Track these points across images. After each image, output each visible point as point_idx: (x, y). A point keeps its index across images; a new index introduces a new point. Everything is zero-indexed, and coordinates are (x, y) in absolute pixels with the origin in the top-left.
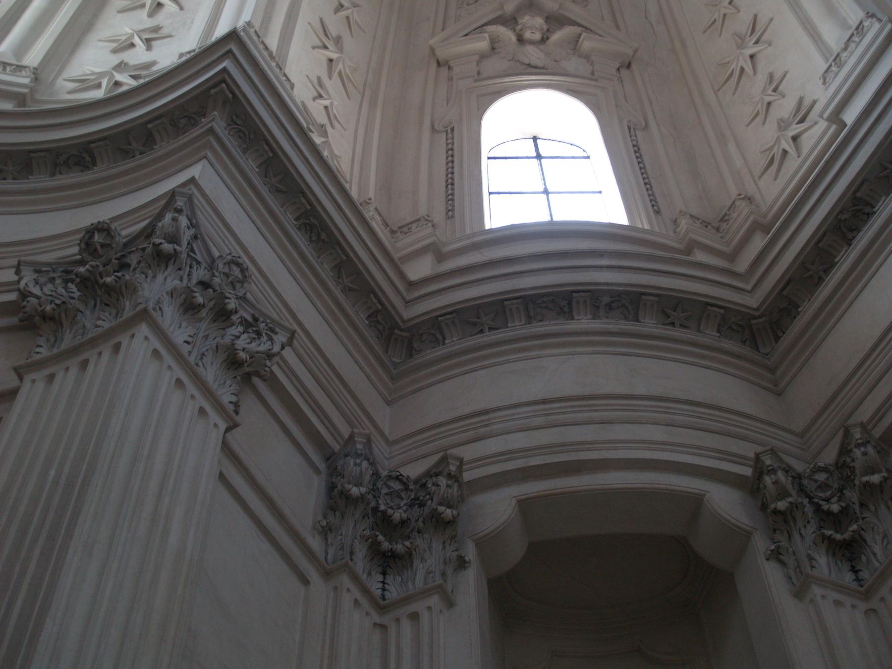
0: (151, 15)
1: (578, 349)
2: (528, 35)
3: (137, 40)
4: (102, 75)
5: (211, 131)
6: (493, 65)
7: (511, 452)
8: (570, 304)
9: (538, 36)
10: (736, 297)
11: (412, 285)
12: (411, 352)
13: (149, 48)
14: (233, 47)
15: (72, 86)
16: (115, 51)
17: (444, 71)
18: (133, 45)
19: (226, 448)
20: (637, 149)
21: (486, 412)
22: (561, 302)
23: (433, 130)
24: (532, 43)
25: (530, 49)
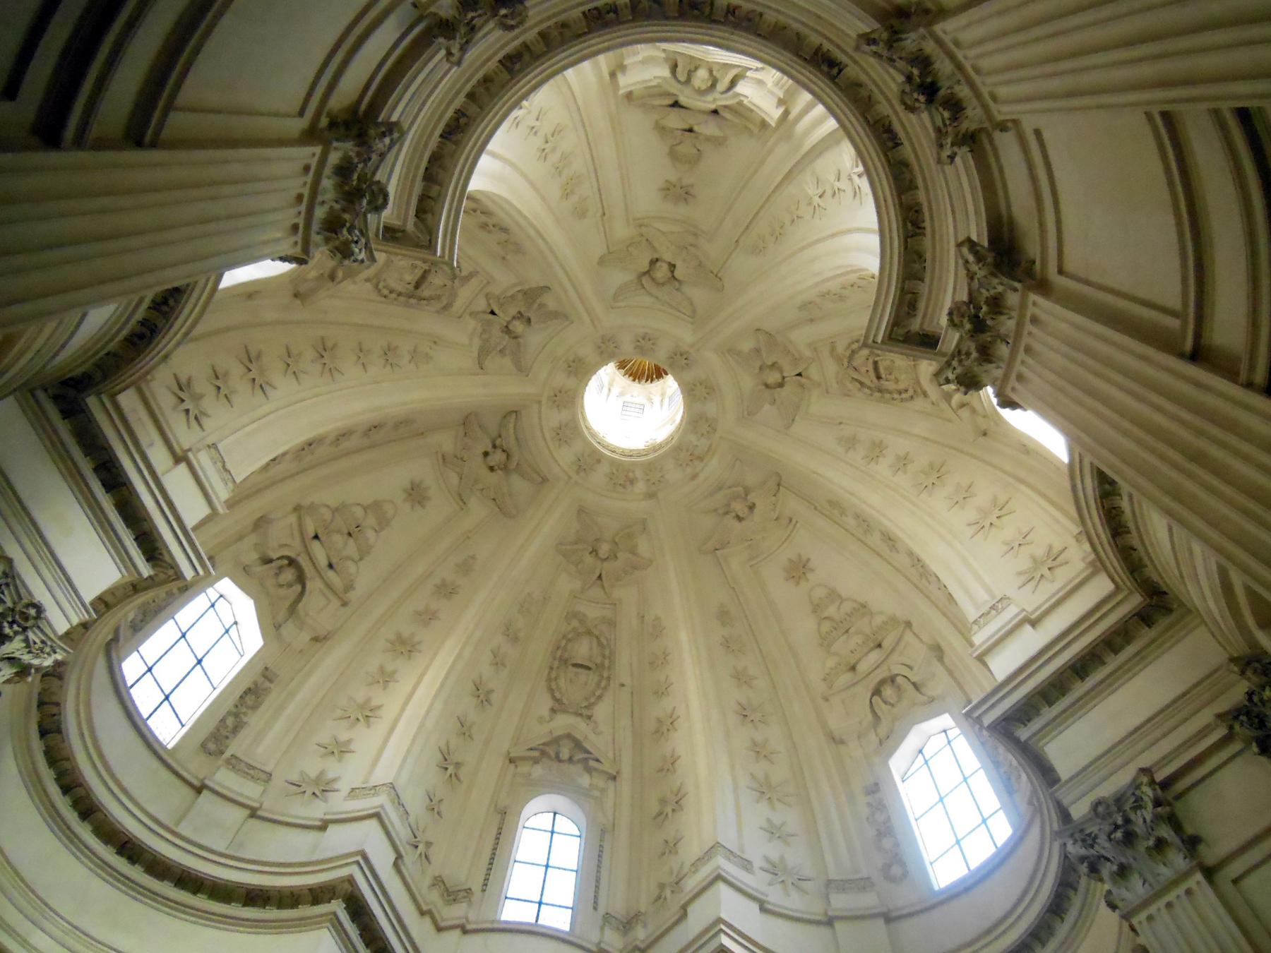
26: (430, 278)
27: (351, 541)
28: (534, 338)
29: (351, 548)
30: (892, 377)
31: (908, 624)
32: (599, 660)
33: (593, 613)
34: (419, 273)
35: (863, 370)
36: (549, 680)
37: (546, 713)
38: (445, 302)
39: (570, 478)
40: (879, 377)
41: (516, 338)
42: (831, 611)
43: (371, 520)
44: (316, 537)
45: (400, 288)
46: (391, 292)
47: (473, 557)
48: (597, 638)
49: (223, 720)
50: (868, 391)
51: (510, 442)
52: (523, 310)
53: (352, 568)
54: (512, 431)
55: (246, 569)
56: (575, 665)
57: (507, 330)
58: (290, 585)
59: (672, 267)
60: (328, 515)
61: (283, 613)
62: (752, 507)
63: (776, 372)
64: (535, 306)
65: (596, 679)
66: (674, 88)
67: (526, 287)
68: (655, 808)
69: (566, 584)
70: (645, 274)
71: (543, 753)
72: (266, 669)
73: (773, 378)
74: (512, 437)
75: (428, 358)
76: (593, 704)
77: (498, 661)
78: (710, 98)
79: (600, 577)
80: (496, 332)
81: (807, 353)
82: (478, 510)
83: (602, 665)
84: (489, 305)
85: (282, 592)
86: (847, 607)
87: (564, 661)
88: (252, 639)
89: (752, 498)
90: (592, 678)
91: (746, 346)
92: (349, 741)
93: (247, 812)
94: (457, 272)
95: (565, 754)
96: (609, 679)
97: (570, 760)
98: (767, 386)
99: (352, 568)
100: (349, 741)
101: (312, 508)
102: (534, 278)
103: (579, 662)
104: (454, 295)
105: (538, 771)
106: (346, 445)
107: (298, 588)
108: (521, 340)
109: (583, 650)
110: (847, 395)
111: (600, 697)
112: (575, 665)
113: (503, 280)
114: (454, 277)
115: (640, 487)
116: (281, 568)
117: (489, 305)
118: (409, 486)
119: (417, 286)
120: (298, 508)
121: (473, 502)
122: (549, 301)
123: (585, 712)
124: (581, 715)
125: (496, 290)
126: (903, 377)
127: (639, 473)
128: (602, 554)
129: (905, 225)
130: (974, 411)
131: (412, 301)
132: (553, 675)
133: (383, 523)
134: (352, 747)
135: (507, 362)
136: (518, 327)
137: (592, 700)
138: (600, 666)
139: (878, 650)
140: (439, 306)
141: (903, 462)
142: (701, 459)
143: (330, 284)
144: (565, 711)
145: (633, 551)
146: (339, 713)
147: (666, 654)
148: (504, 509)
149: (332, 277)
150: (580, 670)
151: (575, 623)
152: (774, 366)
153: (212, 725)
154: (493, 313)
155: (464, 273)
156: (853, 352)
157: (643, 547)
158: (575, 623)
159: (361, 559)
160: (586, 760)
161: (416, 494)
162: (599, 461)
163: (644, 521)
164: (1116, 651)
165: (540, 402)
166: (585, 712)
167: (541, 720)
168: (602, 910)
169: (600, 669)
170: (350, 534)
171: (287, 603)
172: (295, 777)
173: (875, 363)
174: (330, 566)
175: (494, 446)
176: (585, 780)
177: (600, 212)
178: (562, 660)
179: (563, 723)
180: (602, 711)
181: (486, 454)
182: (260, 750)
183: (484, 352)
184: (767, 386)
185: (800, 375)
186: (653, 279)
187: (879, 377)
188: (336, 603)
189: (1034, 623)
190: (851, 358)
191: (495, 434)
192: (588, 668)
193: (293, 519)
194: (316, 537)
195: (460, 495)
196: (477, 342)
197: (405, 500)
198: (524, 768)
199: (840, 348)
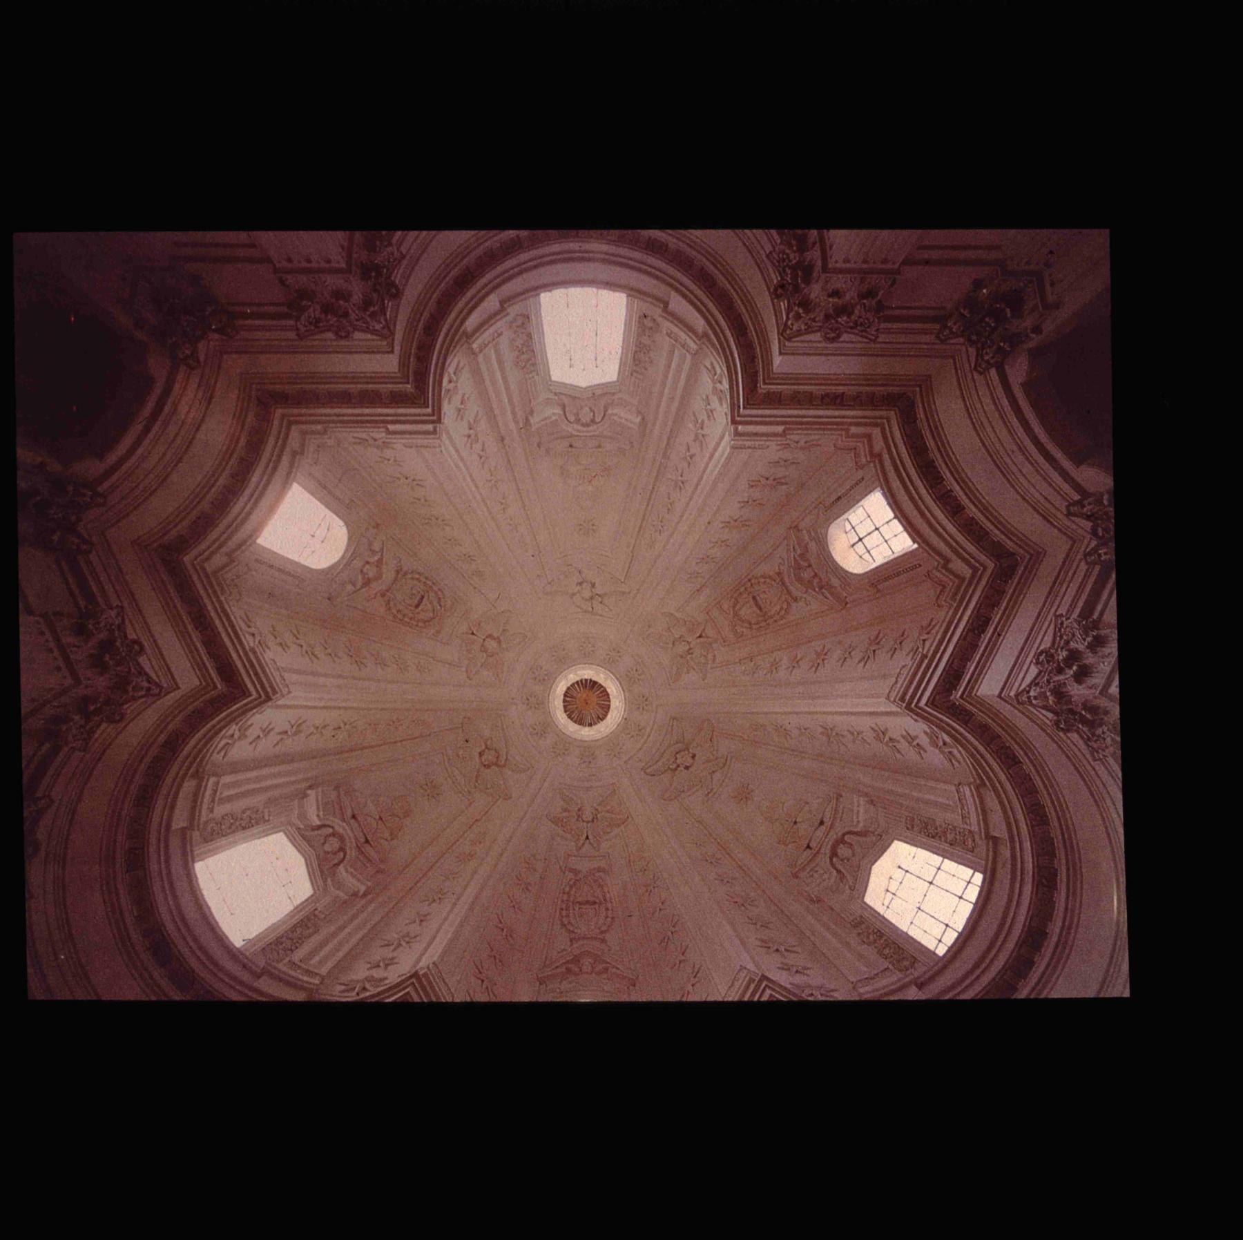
2: (367, 566)
15: (461, 365)
19: (268, 260)
21: (209, 403)
37: (801, 604)
40: (423, 597)
54: (660, 763)
56: (760, 609)
65: (757, 587)
66: (352, 854)
70: (496, 765)
71: (821, 588)
73: (491, 645)
76: (770, 577)
77: (795, 663)
78: (341, 831)
95: (806, 575)
97: (810, 566)
98: (499, 642)
103: (755, 609)
105: (835, 582)
109: (747, 611)
111: (764, 576)
130: (370, 544)
132: (777, 617)
136: (587, 815)
144: (789, 592)
151: (739, 629)
152: (484, 649)
155: (571, 875)
158: (739, 629)
168: (860, 474)
173: (417, 606)
176: (813, 546)
181: (687, 768)
184: (499, 642)
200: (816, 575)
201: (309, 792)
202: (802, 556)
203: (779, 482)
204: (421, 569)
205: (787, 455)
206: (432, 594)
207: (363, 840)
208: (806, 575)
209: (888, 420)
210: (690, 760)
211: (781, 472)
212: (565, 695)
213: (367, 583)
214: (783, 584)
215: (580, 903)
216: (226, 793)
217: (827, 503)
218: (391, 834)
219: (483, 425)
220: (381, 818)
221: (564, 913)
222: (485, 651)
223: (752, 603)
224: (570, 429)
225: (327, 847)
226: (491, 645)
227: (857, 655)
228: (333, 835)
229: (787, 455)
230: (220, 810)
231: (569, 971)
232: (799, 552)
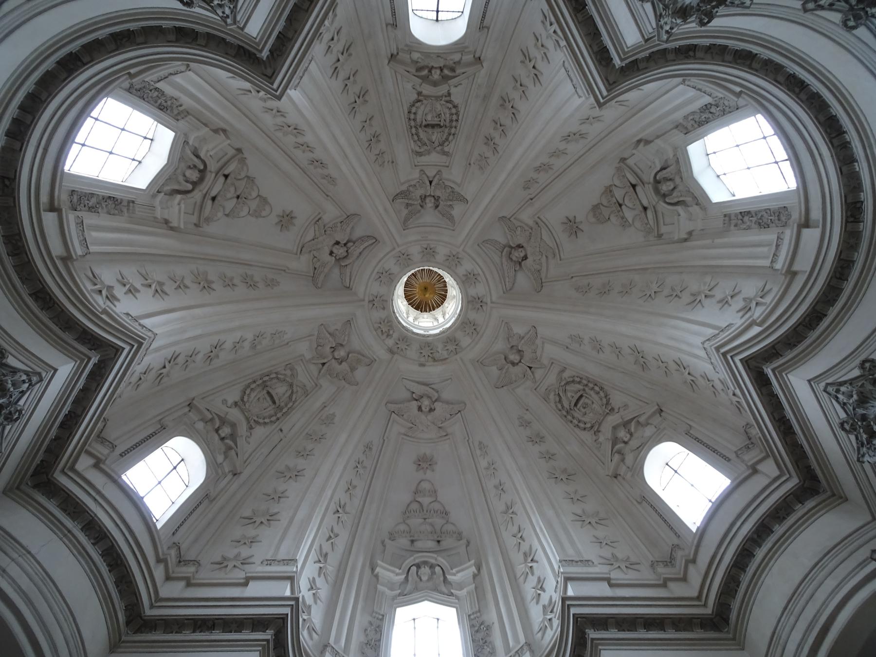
0: (533, 574)
1: (770, 565)
2: (626, 440)
3: (539, 592)
4: (543, 621)
5: (593, 639)
6: (629, 459)
7: (799, 645)
8: (748, 550)
9: (628, 436)
10: (789, 485)
11: (699, 598)
12: (726, 621)
13: (544, 591)
14: (568, 603)
15: (540, 635)
16: (537, 603)
17: (619, 477)
18: (539, 594)
20: (697, 439)
21: (774, 633)
22: (744, 555)
23: (639, 503)
24: (630, 440)
25: (631, 443)
26: (437, 130)
27: (235, 200)
28: (429, 216)
29: (230, 205)
30: (583, 410)
31: (468, 543)
32: (282, 404)
33: (302, 377)
34: (436, 121)
35: (569, 394)
36: (248, 386)
37: (230, 401)
38: (422, 150)
39: (364, 300)
40: (576, 405)
41: (422, 206)
42: (426, 500)
43: (253, 205)
44: (226, 176)
45: (419, 117)
46: (415, 114)
47: (278, 283)
48: (292, 392)
49: (92, 194)
50: (560, 407)
51: (355, 251)
52: (442, 198)
53: (220, 214)
54: (362, 247)
55: (186, 142)
56: (268, 393)
57: (423, 198)
58: (187, 181)
59: (525, 258)
60: (243, 175)
61: (168, 188)
62: (431, 410)
63: (517, 359)
64: (450, 203)
65: (272, 412)
67: (457, 189)
68: (247, 513)
69: (304, 349)
70: (511, 247)
71: (212, 420)
72: (133, 202)
73: (514, 357)
74: (359, 251)
75: (382, 165)
79: (323, 364)
80: (420, 192)
81: (545, 361)
82: (302, 263)
83: (282, 409)
84: (434, 177)
85: (181, 178)
86: (436, 506)
87: (264, 385)
88: (141, 180)
89: (438, 405)
90: (271, 410)
91: (519, 330)
92: (138, 291)
93: (65, 254)
94: (446, 144)
95: (226, 431)
96: (278, 419)
97: (222, 439)
99: (220, 214)
100: (138, 291)
101: (243, 161)
102: (469, 191)
104: (429, 153)
105: (200, 425)
106: (298, 154)
107: (190, 187)
108: (422, 211)
109: (280, 390)
110: (546, 399)
111: (265, 423)
112: (268, 393)
113: (454, 175)
114: (441, 144)
115: (390, 342)
116: (195, 166)
117: (434, 177)
118: (288, 213)
119: (426, 126)
120: (239, 150)
121: (305, 258)
122: (457, 210)
123: (252, 422)
124: (248, 422)
125: (445, 175)
126: (591, 414)
127: (395, 335)
128: (336, 354)
129: (805, 318)
130: (623, 460)
131: (414, 130)
132: (253, 386)
133: (257, 214)
134: (137, 295)
135: (405, 212)
136: (430, 203)
137: (261, 421)
138: (280, 408)
139: (436, 543)
140: (417, 149)
141: (549, 456)
142: (435, 360)
143: (413, 70)
144: (242, 411)
145: (353, 369)
146: (144, 272)
147: (322, 437)
148: (315, 277)
149: (419, 69)
150: (268, 399)
152: (520, 352)
153: (87, 189)
154: (431, 182)
155: (446, 149)
156: (573, 381)
157: (360, 373)
158: (289, 372)
159: (227, 215)
160: (230, 448)
161: (286, 220)
162: (384, 309)
163: (372, 361)
164: (678, 629)
165: (394, 249)
166: (252, 422)
167: (224, 402)
168: (176, 539)
169: (280, 409)
170: (238, 197)
171: (176, 187)
172: (97, 271)
173: (581, 396)
174: (214, 199)
175: (345, 244)
176: (220, 458)
177: (532, 196)
178: (263, 384)
179: (235, 414)
180: (260, 432)
181: (337, 243)
182: (94, 234)
183: (403, 194)
184: (505, 359)
185: (530, 368)
186: (510, 253)
187: (576, 405)
188: (194, 219)
189: (611, 585)
190: (567, 383)
191: (354, 239)
192: (274, 402)
193: (231, 152)
194: (226, 176)
195: (303, 247)
196: (404, 188)
197: (278, 216)
198: (193, 416)
199: (566, 375)
200: (217, 431)
201: (686, 236)
202: (230, 448)
203: (250, 520)
204: (576, 430)
205: (245, 552)
206: (566, 405)
207: (638, 189)
208: (226, 431)
209: (152, 606)
210: (335, 251)
211: (251, 532)
212: (446, 296)
213: (626, 424)
214: (247, 419)
215: (439, 126)
216: (765, 249)
217: (206, 502)
218: (611, 191)
219: (520, 568)
220: (620, 205)
221: (455, 117)
222: (519, 351)
223: (276, 398)
224: (441, 560)
225: (671, 185)
226: (514, 357)
227: (181, 360)
228: (664, 196)
229: (245, 552)
230: (770, 236)
231: (453, 70)
232: (233, 453)
